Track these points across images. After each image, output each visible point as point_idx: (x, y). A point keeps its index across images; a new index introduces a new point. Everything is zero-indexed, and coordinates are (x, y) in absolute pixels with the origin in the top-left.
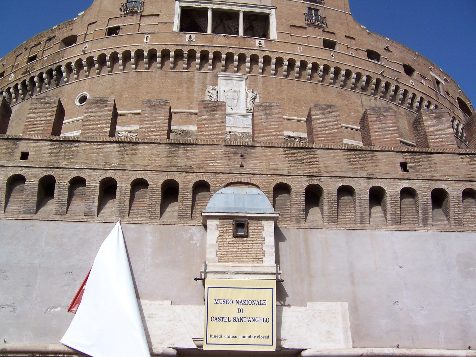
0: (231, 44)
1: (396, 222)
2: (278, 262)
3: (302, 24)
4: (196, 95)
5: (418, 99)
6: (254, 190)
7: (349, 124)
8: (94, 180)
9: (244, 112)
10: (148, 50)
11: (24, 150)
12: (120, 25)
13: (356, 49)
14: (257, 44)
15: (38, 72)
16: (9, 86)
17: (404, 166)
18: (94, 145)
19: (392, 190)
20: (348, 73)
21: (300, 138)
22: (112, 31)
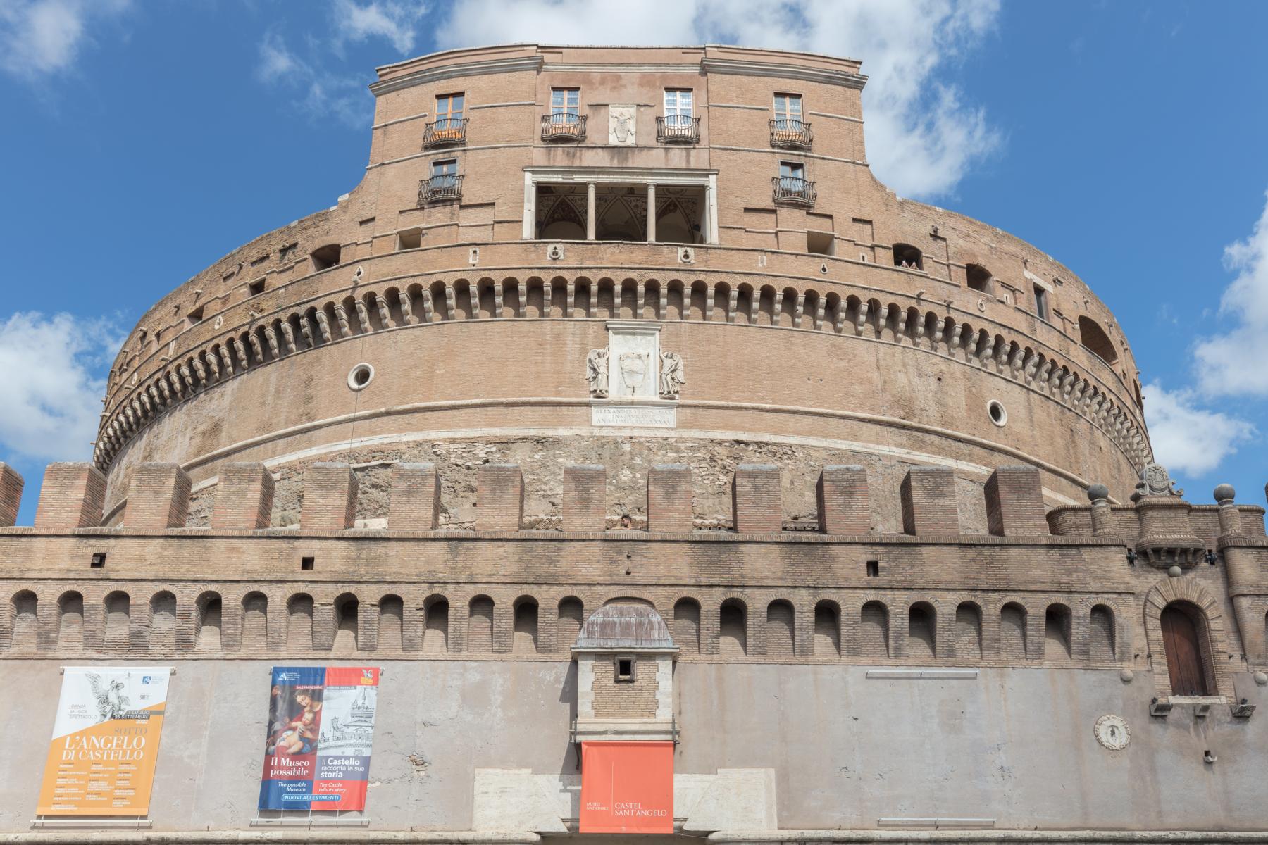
1: (855, 653)
4: (568, 368)
7: (849, 409)
8: (414, 598)
9: (657, 399)
10: (477, 280)
11: (307, 554)
17: (873, 567)
18: (411, 544)
19: (850, 605)
21: (756, 443)
22: (410, 241)
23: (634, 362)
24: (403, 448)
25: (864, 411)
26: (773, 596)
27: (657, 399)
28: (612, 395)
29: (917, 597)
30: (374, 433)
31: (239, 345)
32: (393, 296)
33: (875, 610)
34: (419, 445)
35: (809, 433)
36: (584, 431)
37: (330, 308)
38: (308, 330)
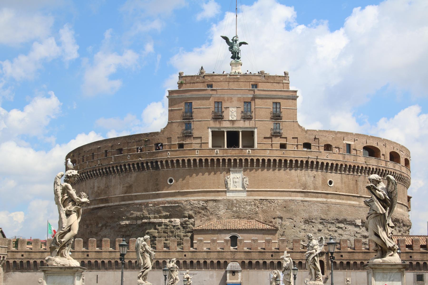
0: (236, 154)
8: (202, 261)
9: (241, 189)
12: (184, 142)
13: (297, 145)
15: (145, 161)
16: (129, 163)
17: (272, 256)
19: (268, 262)
21: (265, 199)
23: (236, 179)
24: (183, 202)
26: (256, 260)
27: (241, 189)
28: (231, 188)
29: (279, 260)
31: (136, 166)
33: (272, 263)
34: (187, 201)
35: (279, 196)
37: (161, 162)
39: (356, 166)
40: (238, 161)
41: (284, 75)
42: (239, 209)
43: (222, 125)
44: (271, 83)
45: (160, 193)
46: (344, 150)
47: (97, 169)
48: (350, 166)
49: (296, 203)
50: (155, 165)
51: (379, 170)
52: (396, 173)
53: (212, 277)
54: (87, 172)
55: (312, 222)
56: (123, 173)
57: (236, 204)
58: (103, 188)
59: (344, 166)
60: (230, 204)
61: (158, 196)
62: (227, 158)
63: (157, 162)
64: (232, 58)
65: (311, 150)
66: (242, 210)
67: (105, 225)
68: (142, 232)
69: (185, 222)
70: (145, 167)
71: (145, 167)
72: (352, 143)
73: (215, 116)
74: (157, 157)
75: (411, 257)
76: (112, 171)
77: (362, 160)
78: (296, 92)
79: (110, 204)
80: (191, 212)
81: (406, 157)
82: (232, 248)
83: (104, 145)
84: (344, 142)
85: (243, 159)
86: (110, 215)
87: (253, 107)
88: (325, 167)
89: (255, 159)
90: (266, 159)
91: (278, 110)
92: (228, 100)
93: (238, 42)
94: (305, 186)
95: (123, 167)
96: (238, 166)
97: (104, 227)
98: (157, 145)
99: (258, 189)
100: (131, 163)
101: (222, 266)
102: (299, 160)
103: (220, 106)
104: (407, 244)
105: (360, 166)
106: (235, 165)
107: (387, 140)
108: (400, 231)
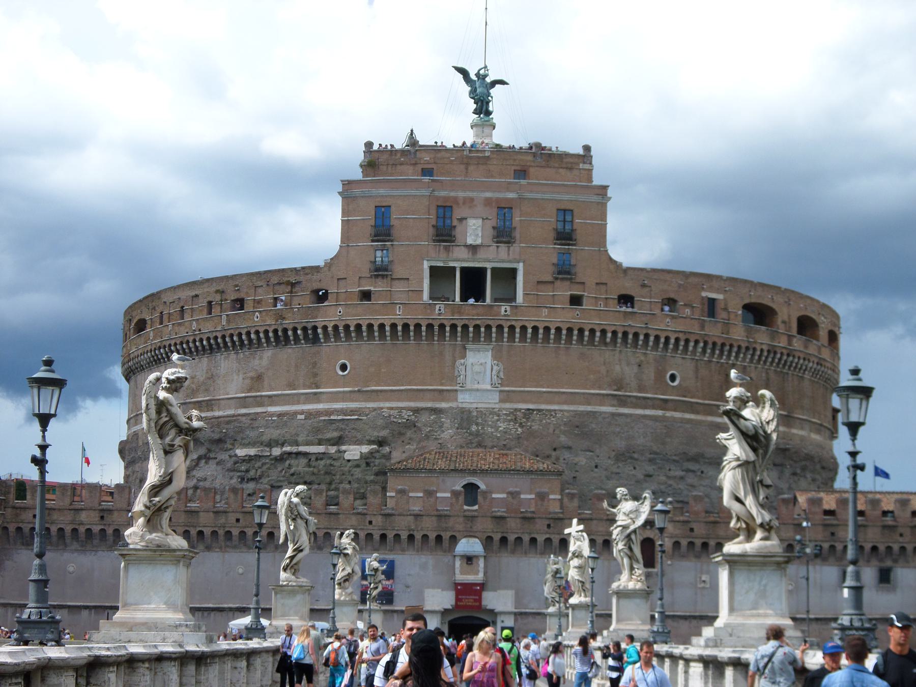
0: (478, 315)
2: (485, 573)
3: (549, 278)
5: (672, 341)
6: (477, 540)
8: (404, 535)
9: (489, 387)
12: (372, 289)
14: (503, 313)
15: (291, 327)
16: (257, 328)
17: (549, 526)
19: (541, 539)
20: (592, 331)
25: (594, 389)
27: (489, 387)
28: (469, 386)
30: (352, 401)
31: (271, 334)
32: (358, 327)
33: (548, 540)
34: (375, 409)
35: (565, 403)
36: (454, 405)
38: (312, 336)
39: (728, 344)
40: (483, 329)
41: (581, 152)
42: (483, 428)
43: (451, 254)
44: (554, 167)
45: (321, 393)
46: (702, 310)
47: (191, 339)
48: (714, 344)
49: (600, 419)
50: (312, 336)
51: (775, 353)
52: (809, 361)
53: (424, 567)
54: (170, 345)
55: (632, 458)
56: (245, 349)
57: (477, 418)
58: (202, 379)
59: (701, 345)
60: (465, 418)
61: (316, 398)
62: (460, 324)
63: (315, 328)
64: (475, 112)
65: (635, 310)
66: (490, 430)
67: (206, 458)
68: (281, 471)
69: (371, 452)
70: (291, 338)
71: (291, 338)
72: (719, 296)
73: (437, 236)
74: (316, 317)
75: (833, 534)
76: (222, 345)
77: (738, 333)
78: (605, 188)
79: (217, 413)
80: (384, 433)
81: (830, 328)
82: (466, 507)
83: (205, 290)
84: (704, 294)
85: (494, 324)
86: (216, 436)
87: (517, 219)
88: (661, 345)
89: (518, 326)
90: (541, 327)
91: (568, 227)
92: (464, 203)
93: (488, 80)
94: (619, 384)
95: (244, 337)
96: (482, 339)
97: (204, 461)
98: (316, 292)
99: (522, 389)
100: (261, 330)
101: (446, 543)
102: (610, 329)
103: (448, 214)
104: (826, 507)
105: (735, 344)
106: (477, 338)
107: (793, 292)
108: (814, 480)
